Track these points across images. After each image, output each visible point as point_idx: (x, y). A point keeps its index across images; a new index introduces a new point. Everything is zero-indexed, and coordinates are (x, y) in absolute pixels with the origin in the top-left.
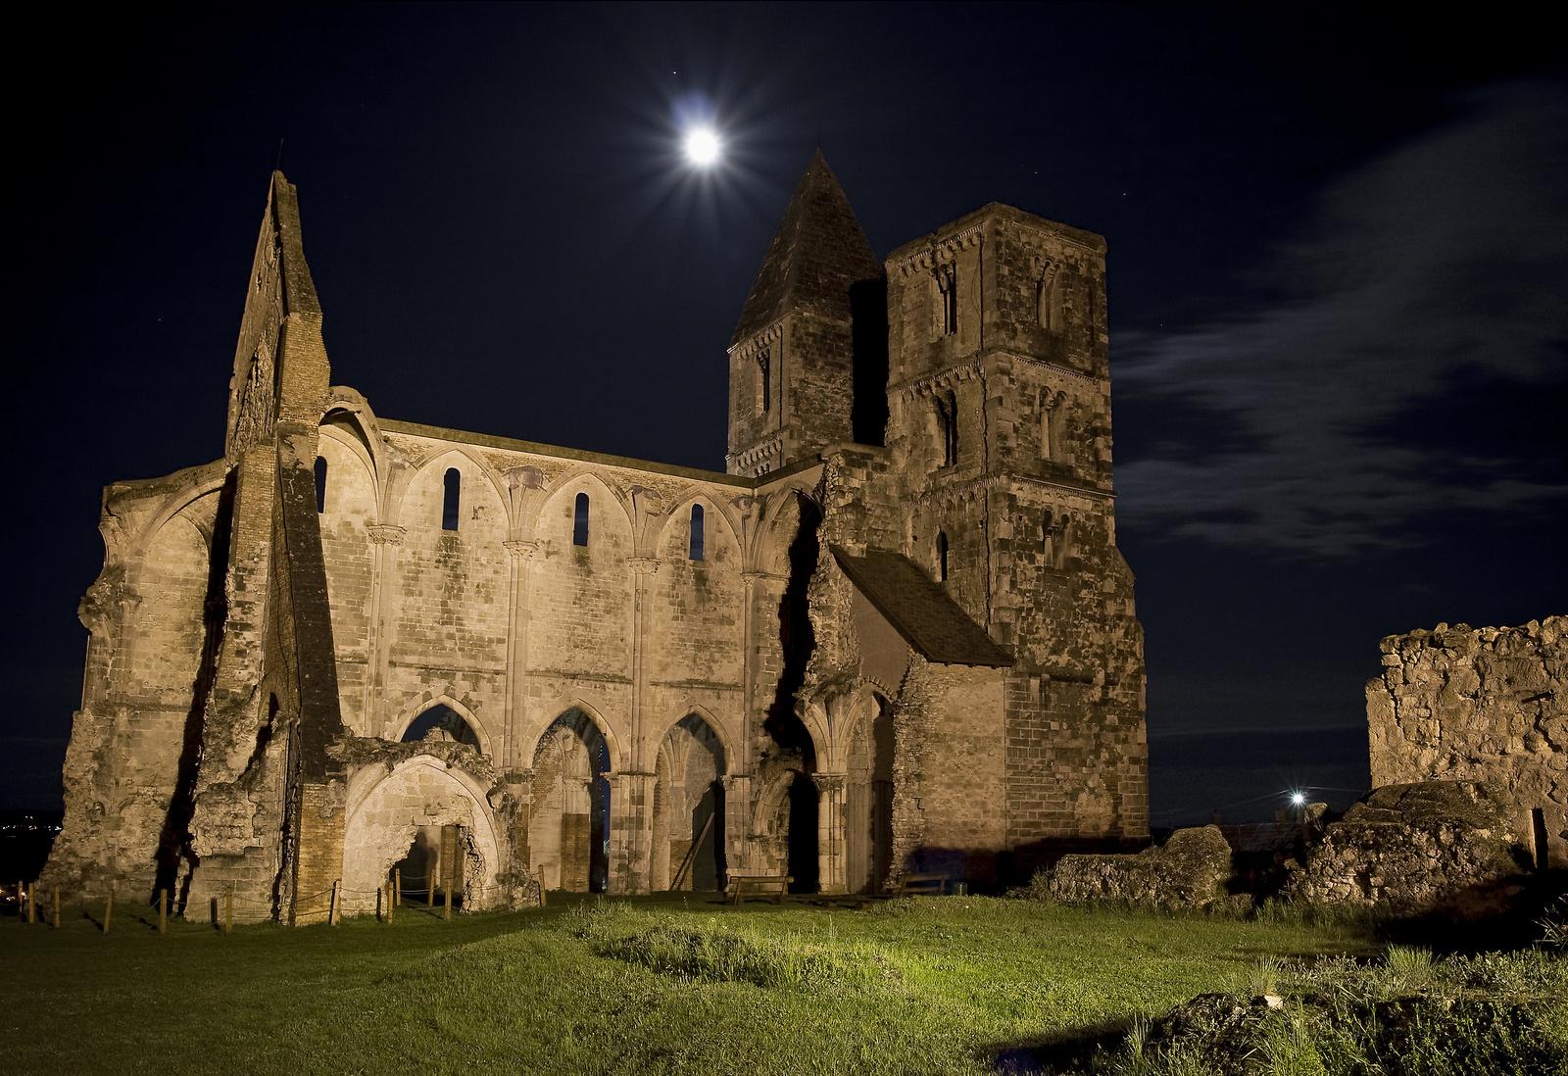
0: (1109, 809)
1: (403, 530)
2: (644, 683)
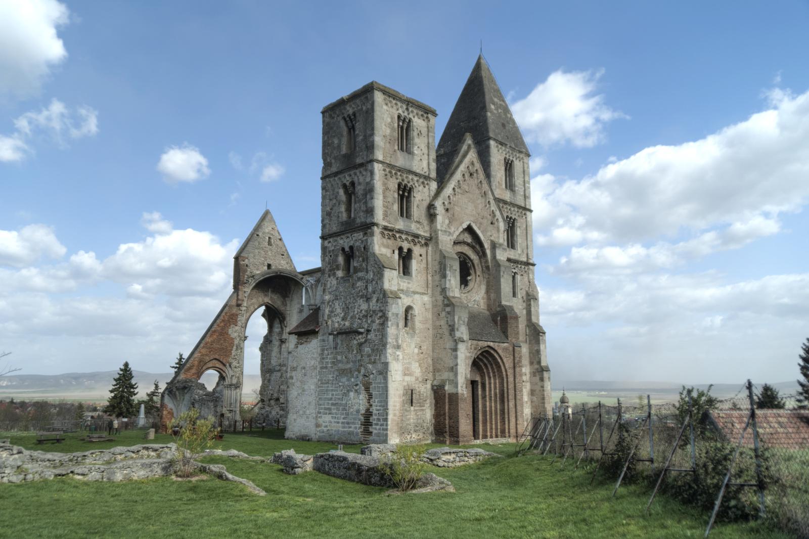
0: (365, 401)
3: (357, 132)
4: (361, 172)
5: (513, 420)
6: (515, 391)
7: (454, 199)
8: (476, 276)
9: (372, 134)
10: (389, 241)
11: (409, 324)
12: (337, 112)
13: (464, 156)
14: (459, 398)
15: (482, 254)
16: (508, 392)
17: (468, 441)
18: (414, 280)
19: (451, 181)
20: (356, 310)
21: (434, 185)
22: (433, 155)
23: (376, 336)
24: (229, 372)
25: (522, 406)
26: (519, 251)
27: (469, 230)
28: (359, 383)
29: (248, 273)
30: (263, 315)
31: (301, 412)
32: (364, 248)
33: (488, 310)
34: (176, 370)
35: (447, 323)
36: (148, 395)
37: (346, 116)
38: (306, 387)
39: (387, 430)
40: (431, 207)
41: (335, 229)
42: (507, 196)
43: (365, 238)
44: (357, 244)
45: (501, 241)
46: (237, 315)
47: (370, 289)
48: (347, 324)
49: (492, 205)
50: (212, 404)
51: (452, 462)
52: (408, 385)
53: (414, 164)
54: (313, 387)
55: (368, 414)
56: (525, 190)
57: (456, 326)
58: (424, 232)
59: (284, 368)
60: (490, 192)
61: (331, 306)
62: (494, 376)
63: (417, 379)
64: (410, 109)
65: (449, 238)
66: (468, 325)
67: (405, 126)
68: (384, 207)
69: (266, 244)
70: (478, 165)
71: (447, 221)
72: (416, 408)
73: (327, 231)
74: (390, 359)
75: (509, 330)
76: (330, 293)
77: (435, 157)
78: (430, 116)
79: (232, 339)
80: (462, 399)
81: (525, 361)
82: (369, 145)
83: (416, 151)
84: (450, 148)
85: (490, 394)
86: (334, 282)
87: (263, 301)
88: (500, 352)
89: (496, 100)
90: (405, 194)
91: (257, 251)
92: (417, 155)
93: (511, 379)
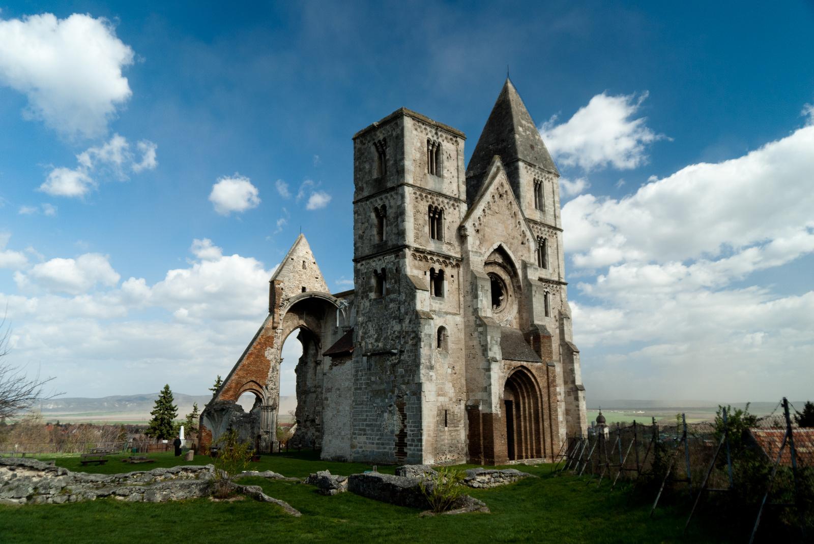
0: (399, 421)
3: (387, 157)
4: (392, 196)
5: (548, 440)
6: (550, 411)
7: (485, 220)
8: (508, 296)
9: (403, 159)
10: (420, 262)
11: (442, 344)
12: (368, 139)
13: (494, 178)
14: (494, 418)
15: (513, 273)
16: (542, 412)
17: (503, 462)
18: (446, 301)
19: (481, 203)
20: (389, 331)
21: (464, 207)
22: (463, 178)
23: (409, 356)
24: (265, 394)
25: (557, 427)
26: (551, 270)
27: (500, 250)
28: (393, 403)
29: (283, 296)
30: (299, 337)
31: (336, 433)
32: (396, 270)
33: (521, 330)
34: (215, 392)
35: (480, 343)
36: (188, 417)
37: (376, 141)
38: (341, 408)
39: (421, 450)
40: (461, 228)
41: (367, 251)
42: (537, 216)
43: (397, 260)
44: (390, 266)
45: (532, 261)
46: (273, 338)
47: (403, 310)
48: (380, 345)
49: (522, 225)
50: (249, 425)
51: (487, 483)
52: (442, 406)
53: (444, 187)
54: (347, 408)
55: (402, 435)
56: (555, 210)
57: (489, 346)
58: (455, 252)
59: (320, 390)
60: (520, 213)
61: (364, 327)
62: (528, 396)
63: (451, 399)
64: (440, 133)
65: (480, 259)
66: (500, 344)
67: (435, 150)
68: (415, 229)
69: (301, 268)
70: (507, 187)
71: (478, 242)
72: (450, 429)
73: (359, 254)
74: (423, 379)
75: (542, 349)
76: (363, 315)
77: (465, 180)
78: (458, 139)
79: (269, 361)
80: (496, 419)
81: (560, 380)
82: (399, 169)
83: (445, 173)
84: (479, 170)
85: (525, 414)
86: (367, 304)
87: (298, 323)
88: (534, 371)
89: (524, 122)
90: (436, 216)
91: (291, 275)
92: (447, 178)
93: (545, 399)
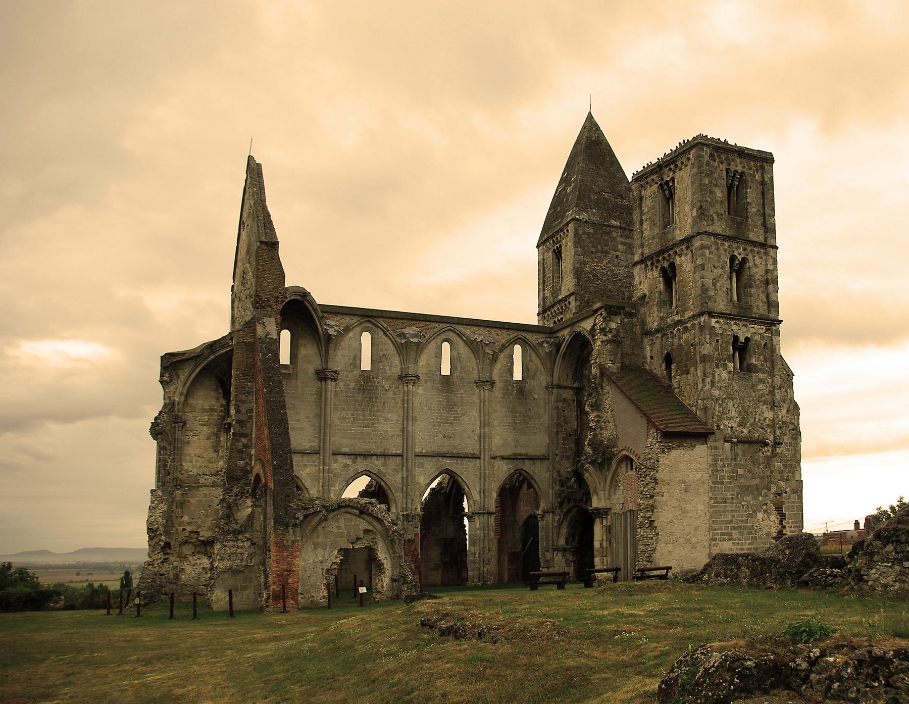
1: (337, 373)
2: (487, 457)
20: (757, 416)
31: (682, 541)
48: (745, 431)
61: (720, 405)
86: (725, 375)
